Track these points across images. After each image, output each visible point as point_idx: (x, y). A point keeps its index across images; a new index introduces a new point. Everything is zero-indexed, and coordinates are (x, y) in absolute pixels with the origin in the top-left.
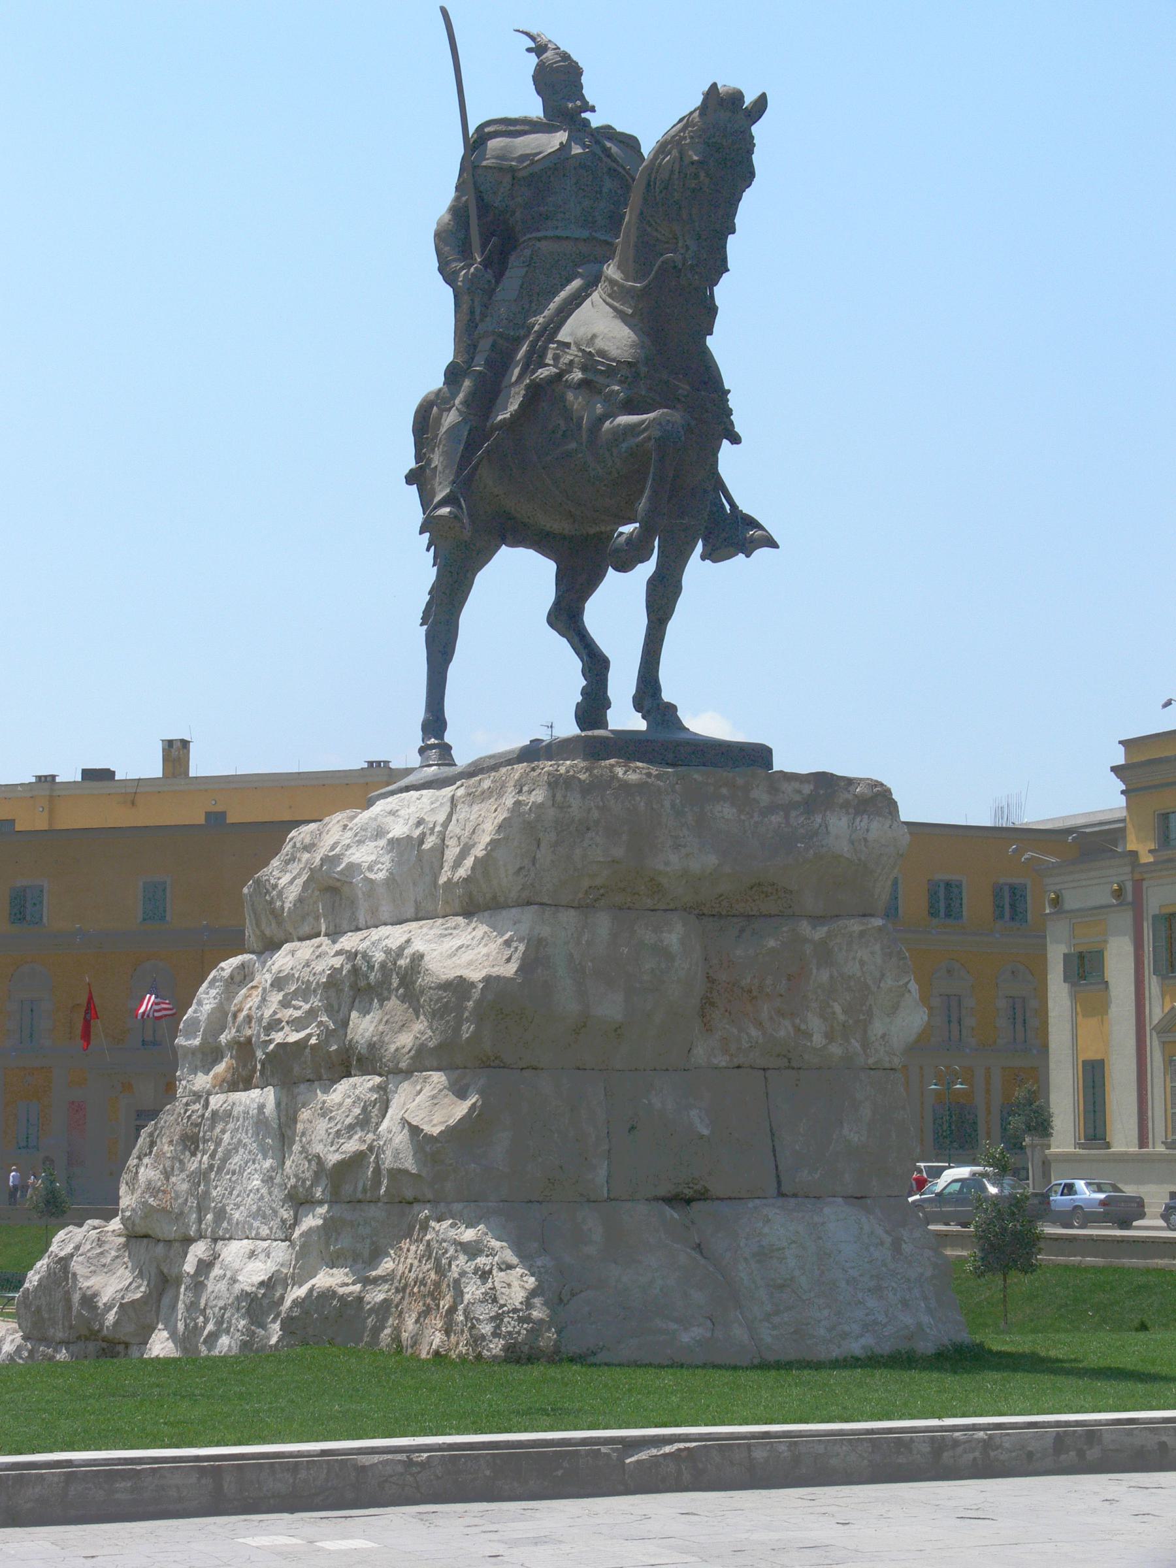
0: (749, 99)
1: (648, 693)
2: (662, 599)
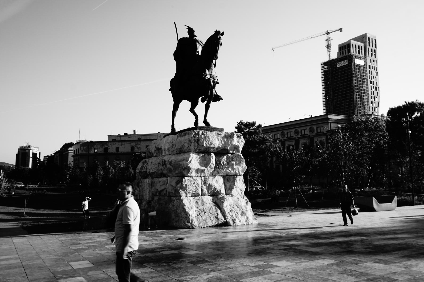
0: (221, 32)
1: (205, 121)
2: (207, 107)
